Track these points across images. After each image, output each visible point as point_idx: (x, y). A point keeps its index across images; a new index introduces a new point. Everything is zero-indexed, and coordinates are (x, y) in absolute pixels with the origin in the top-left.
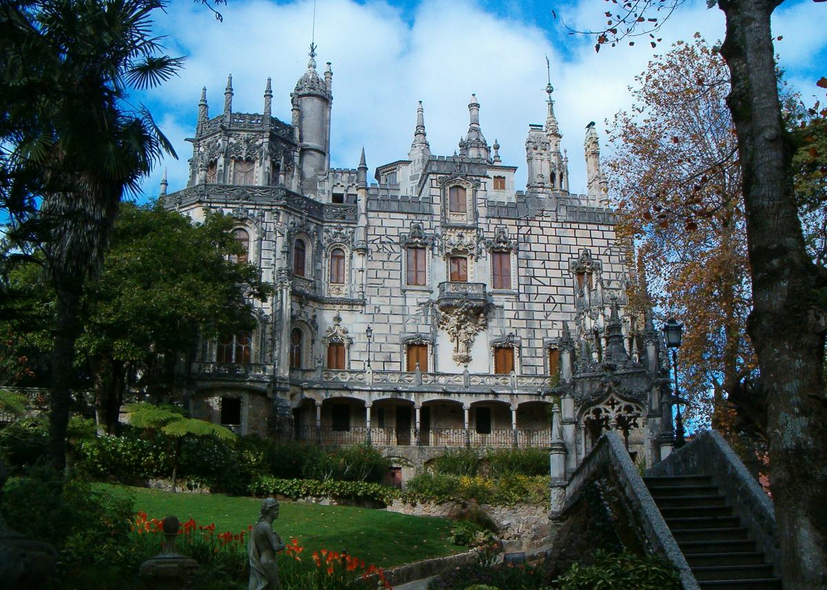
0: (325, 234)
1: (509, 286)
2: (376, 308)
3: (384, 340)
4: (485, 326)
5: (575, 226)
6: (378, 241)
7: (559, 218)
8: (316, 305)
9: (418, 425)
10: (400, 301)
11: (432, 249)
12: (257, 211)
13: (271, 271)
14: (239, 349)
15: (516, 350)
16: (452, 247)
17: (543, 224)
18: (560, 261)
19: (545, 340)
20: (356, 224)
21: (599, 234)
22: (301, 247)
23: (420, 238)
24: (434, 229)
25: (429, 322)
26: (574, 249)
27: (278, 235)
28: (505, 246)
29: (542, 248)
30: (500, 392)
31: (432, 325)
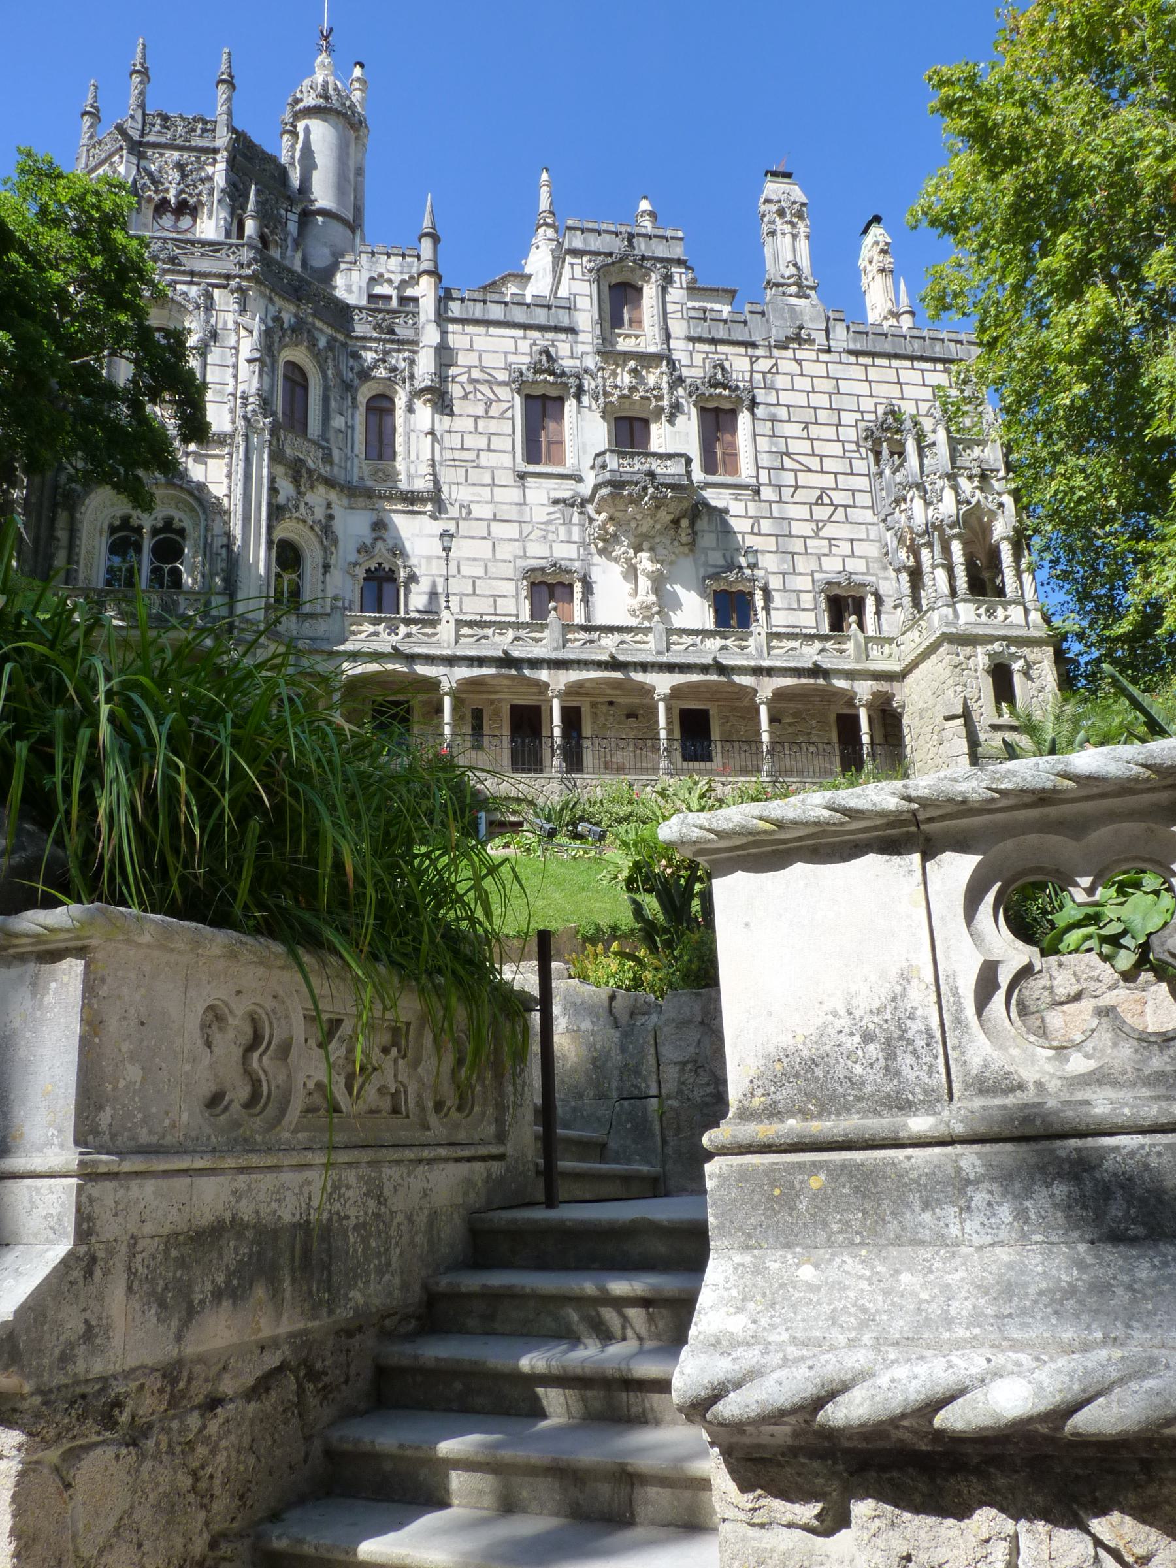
0: (351, 362)
1: (735, 471)
2: (461, 506)
3: (481, 572)
4: (692, 545)
5: (868, 361)
6: (464, 378)
7: (832, 343)
8: (333, 495)
9: (557, 732)
10: (514, 494)
11: (578, 397)
12: (194, 288)
13: (227, 407)
14: (156, 571)
15: (759, 597)
16: (617, 392)
17: (800, 354)
18: (840, 424)
19: (817, 576)
20: (417, 343)
21: (916, 377)
22: (299, 379)
23: (552, 373)
24: (581, 358)
25: (576, 538)
26: (867, 404)
27: (243, 333)
28: (727, 392)
29: (801, 399)
30: (732, 663)
31: (583, 544)
